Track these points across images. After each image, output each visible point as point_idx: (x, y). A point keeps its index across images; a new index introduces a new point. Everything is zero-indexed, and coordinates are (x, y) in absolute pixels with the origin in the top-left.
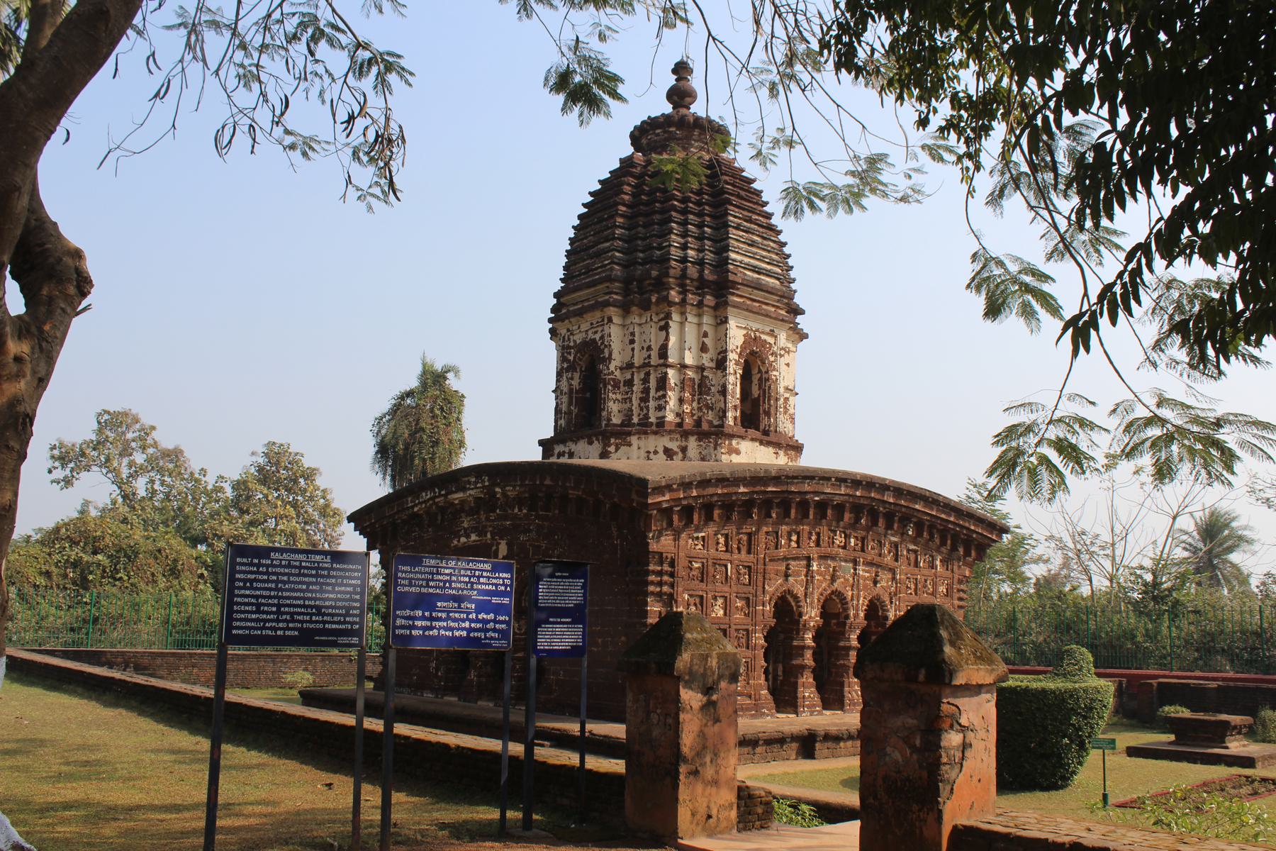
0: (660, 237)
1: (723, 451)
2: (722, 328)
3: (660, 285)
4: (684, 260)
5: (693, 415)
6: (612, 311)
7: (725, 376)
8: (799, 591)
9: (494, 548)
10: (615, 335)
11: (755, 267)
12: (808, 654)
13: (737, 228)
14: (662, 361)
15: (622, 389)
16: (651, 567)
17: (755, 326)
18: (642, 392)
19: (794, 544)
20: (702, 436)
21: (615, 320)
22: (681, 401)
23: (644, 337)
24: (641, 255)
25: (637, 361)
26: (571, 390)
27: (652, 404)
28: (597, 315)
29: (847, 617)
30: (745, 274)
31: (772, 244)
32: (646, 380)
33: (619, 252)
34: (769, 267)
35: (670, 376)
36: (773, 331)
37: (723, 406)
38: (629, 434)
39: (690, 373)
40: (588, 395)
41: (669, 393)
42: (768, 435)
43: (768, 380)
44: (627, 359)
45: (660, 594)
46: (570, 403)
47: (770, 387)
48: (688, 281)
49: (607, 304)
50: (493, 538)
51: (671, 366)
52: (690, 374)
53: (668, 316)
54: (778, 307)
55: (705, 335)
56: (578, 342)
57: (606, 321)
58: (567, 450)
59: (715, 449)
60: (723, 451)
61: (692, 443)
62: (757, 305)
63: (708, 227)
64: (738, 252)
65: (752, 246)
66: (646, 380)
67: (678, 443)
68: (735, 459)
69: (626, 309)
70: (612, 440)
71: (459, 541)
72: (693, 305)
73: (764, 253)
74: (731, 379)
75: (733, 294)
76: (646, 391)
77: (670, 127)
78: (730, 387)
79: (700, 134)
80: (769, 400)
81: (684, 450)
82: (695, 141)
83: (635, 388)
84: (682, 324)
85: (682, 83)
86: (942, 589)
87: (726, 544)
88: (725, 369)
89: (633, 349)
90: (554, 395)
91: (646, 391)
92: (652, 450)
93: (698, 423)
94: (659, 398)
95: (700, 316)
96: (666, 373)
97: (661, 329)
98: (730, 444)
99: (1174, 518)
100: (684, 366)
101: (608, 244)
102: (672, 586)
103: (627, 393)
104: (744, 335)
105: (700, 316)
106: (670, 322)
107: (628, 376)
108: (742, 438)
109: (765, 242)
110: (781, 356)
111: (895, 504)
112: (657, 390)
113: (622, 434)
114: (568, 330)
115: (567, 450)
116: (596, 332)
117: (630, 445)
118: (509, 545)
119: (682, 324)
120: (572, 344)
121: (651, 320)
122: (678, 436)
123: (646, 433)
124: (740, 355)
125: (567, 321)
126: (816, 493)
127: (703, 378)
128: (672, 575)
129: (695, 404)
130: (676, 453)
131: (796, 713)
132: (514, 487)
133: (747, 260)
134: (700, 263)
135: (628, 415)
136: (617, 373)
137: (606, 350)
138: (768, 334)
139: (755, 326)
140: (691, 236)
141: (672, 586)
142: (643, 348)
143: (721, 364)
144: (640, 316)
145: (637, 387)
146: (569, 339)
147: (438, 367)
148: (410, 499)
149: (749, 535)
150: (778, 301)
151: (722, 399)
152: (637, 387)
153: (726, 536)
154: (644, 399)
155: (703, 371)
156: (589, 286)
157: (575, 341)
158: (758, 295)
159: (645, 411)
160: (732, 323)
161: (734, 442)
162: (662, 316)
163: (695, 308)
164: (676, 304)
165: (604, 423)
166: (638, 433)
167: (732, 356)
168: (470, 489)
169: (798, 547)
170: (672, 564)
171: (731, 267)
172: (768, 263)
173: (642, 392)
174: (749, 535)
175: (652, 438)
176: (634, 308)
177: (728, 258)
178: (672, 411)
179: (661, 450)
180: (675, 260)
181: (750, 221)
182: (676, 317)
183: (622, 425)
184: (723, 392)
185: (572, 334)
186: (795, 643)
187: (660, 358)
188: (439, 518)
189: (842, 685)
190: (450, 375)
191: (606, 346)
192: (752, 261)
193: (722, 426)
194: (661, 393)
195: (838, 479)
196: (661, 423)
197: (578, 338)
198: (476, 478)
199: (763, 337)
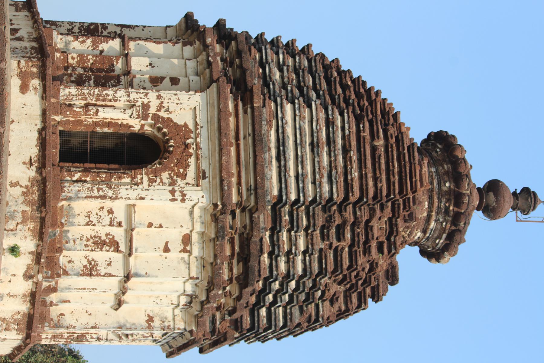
1: (23, 62)
4: (262, 65)
5: (66, 68)
13: (329, 123)
17: (203, 140)
22: (81, 56)
30: (269, 123)
31: (326, 188)
34: (292, 173)
35: (111, 43)
36: (204, 177)
39: (120, 62)
41: (89, 41)
47: (124, 173)
48: (237, 60)
51: (124, 44)
52: (119, 66)
54: (239, 184)
59: (24, 57)
60: (23, 62)
61: (27, 44)
62: (233, 141)
64: (295, 115)
65: (312, 150)
67: (26, 36)
68: (14, 83)
73: (309, 168)
74: (121, 94)
75: (235, 100)
77: (440, 144)
78: (110, 92)
79: (447, 173)
80: (105, 172)
81: (20, 39)
82: (437, 171)
85: (509, 201)
95: (197, 74)
98: (33, 76)
104: (186, 125)
106: (179, 46)
109: (325, 175)
110: (173, 192)
122: (35, 36)
124: (156, 117)
129: (80, 71)
133: (289, 131)
134: (266, 81)
138: (198, 167)
140: (299, 81)
150: (248, 189)
155: (124, 75)
158: (246, 145)
161: (36, 82)
163: (205, 64)
167: (153, 95)
171: (273, 105)
172: (297, 177)
178: (67, 44)
180: (261, 57)
181: (346, 150)
182: (188, 50)
192: (290, 143)
199: (192, 161)
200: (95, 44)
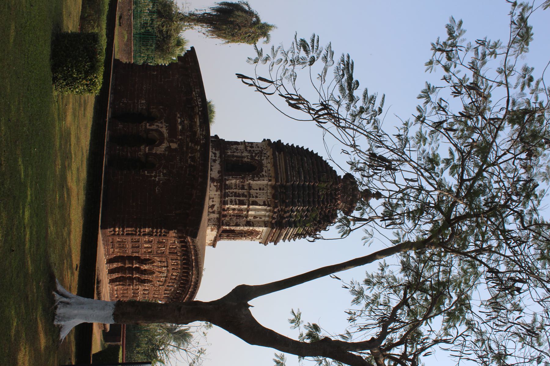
0: (303, 201)
1: (212, 227)
2: (263, 225)
3: (283, 202)
4: (292, 211)
6: (273, 182)
7: (243, 226)
8: (155, 264)
9: (175, 140)
10: (264, 182)
11: (288, 234)
12: (131, 265)
14: (251, 202)
15: (241, 184)
16: (163, 230)
17: (263, 234)
18: (239, 193)
19: (173, 263)
20: (219, 219)
21: (270, 183)
22: (234, 209)
23: (262, 194)
24: (296, 193)
25: (252, 191)
26: (243, 157)
27: (233, 198)
28: (273, 174)
29: (145, 275)
32: (243, 195)
33: (299, 183)
37: (231, 225)
38: (221, 191)
40: (240, 164)
42: (219, 236)
43: (242, 237)
44: (253, 187)
45: (152, 232)
46: (237, 157)
49: (277, 181)
50: (179, 140)
53: (269, 206)
55: (260, 218)
56: (263, 161)
57: (270, 178)
58: (217, 158)
59: (213, 224)
61: (216, 216)
63: (305, 219)
66: (243, 195)
67: (216, 210)
69: (273, 187)
70: (219, 184)
71: (179, 118)
72: (273, 215)
74: (242, 228)
75: (277, 229)
76: (239, 196)
80: (233, 237)
81: (213, 212)
82: (345, 205)
83: (240, 190)
84: (265, 210)
86: (156, 296)
87: (172, 248)
88: (246, 226)
89: (257, 190)
90: (243, 141)
91: (239, 196)
92: (214, 200)
93: (225, 216)
94: (235, 201)
96: (245, 205)
97: (264, 202)
99: (185, 350)
100: (248, 211)
101: (303, 178)
102: (156, 235)
103: (239, 187)
105: (269, 216)
107: (246, 187)
108: (218, 232)
111: (188, 291)
112: (239, 200)
113: (222, 187)
114: (269, 156)
115: (217, 158)
116: (266, 172)
117: (217, 191)
118: (175, 150)
119: (265, 210)
120: (263, 158)
121: (268, 198)
122: (219, 210)
123: (221, 198)
125: (272, 157)
126: (192, 274)
127: (243, 217)
128: (160, 235)
129: (232, 214)
130: (212, 209)
131: (107, 263)
132: (199, 158)
134: (290, 216)
135: (229, 187)
136: (247, 182)
137: (257, 179)
139: (263, 234)
141: (156, 235)
142: (257, 194)
143: (249, 224)
144: (271, 193)
145: (241, 191)
146: (265, 156)
147: (270, 33)
148: (198, 90)
149: (176, 253)
151: (234, 224)
152: (241, 191)
153: (176, 248)
154: (236, 195)
156: (286, 169)
157: (263, 160)
159: (231, 195)
160: (265, 229)
162: (270, 203)
164: (274, 209)
165: (226, 177)
166: (221, 195)
168: (200, 130)
169: (172, 265)
170: (164, 235)
173: (239, 193)
174: (176, 253)
175: (219, 200)
176: (273, 192)
177: (292, 227)
179: (214, 203)
180: (292, 208)
182: (269, 208)
183: (226, 185)
184: (237, 225)
185: (267, 159)
186: (134, 261)
187: (252, 202)
188: (190, 106)
189: (119, 273)
190: (265, 39)
191: (259, 178)
193: (223, 225)
194: (238, 202)
195: (197, 281)
196: (225, 203)
197: (264, 162)
198: (205, 135)
200: (239, 207)
